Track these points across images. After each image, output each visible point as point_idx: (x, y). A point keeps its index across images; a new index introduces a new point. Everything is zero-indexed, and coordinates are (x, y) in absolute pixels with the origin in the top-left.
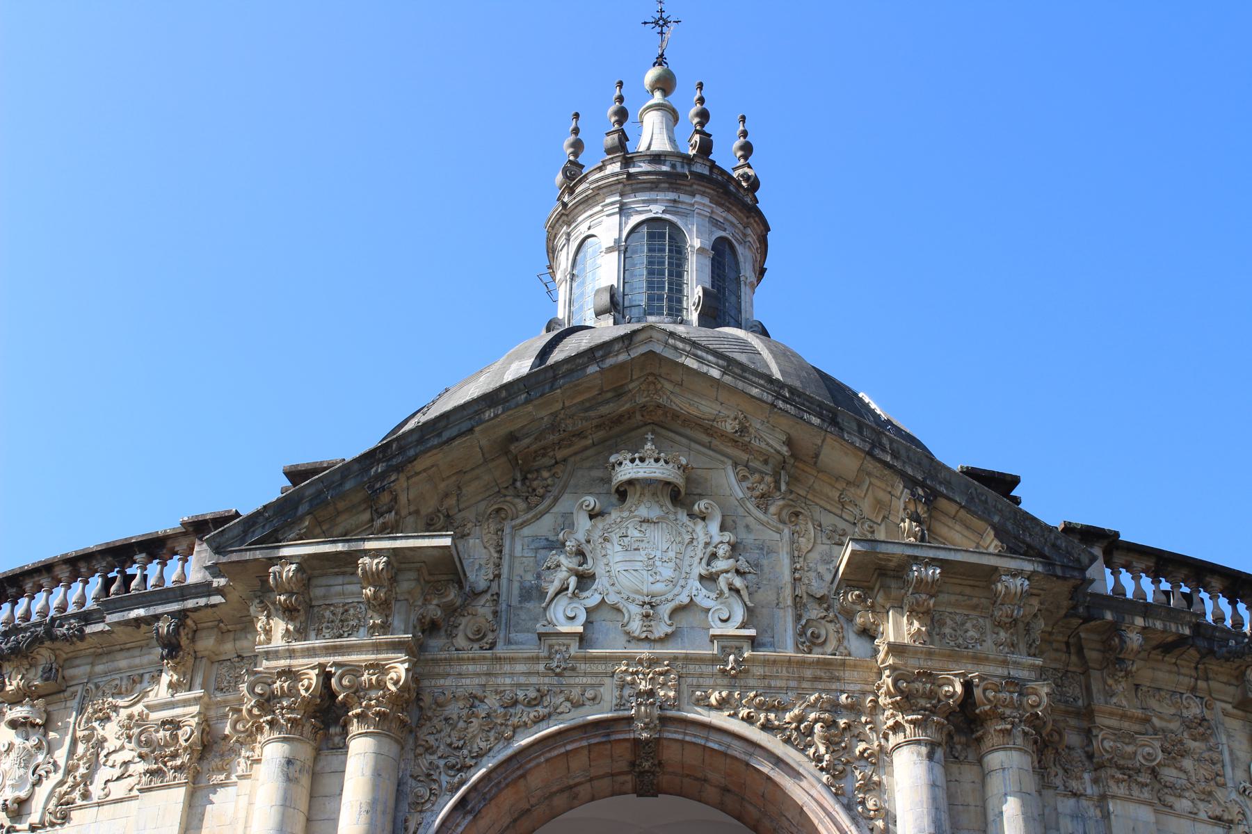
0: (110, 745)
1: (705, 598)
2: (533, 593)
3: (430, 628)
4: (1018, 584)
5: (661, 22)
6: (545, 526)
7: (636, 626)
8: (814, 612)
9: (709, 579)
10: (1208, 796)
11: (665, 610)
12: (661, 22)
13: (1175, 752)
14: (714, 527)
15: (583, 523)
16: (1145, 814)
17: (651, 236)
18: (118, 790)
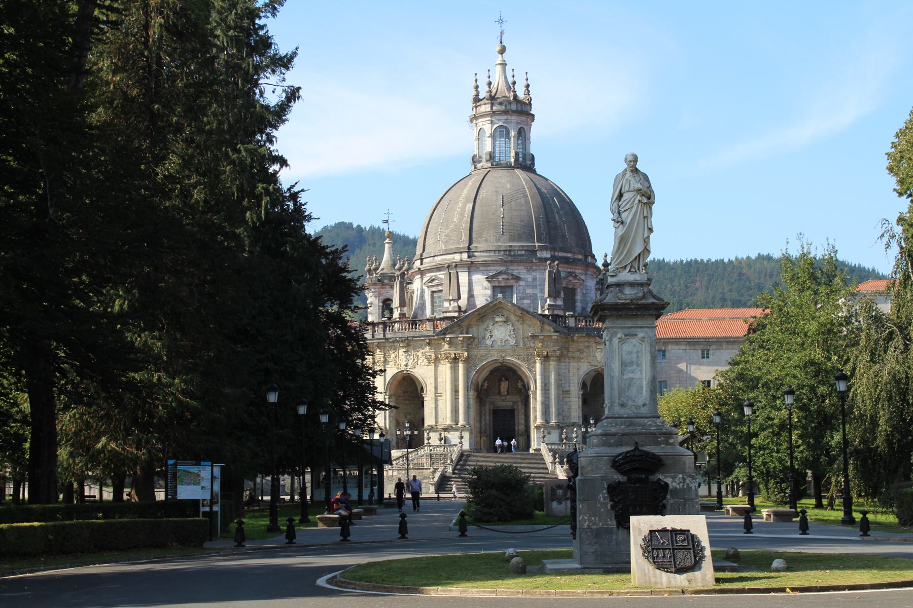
0: (420, 356)
1: (509, 339)
2: (484, 338)
3: (469, 344)
4: (556, 337)
5: (501, 21)
6: (485, 326)
7: (499, 344)
8: (526, 340)
9: (510, 335)
10: (587, 359)
11: (503, 341)
12: (501, 21)
13: (582, 353)
14: (511, 326)
15: (491, 326)
16: (576, 364)
17: (500, 131)
18: (423, 364)
